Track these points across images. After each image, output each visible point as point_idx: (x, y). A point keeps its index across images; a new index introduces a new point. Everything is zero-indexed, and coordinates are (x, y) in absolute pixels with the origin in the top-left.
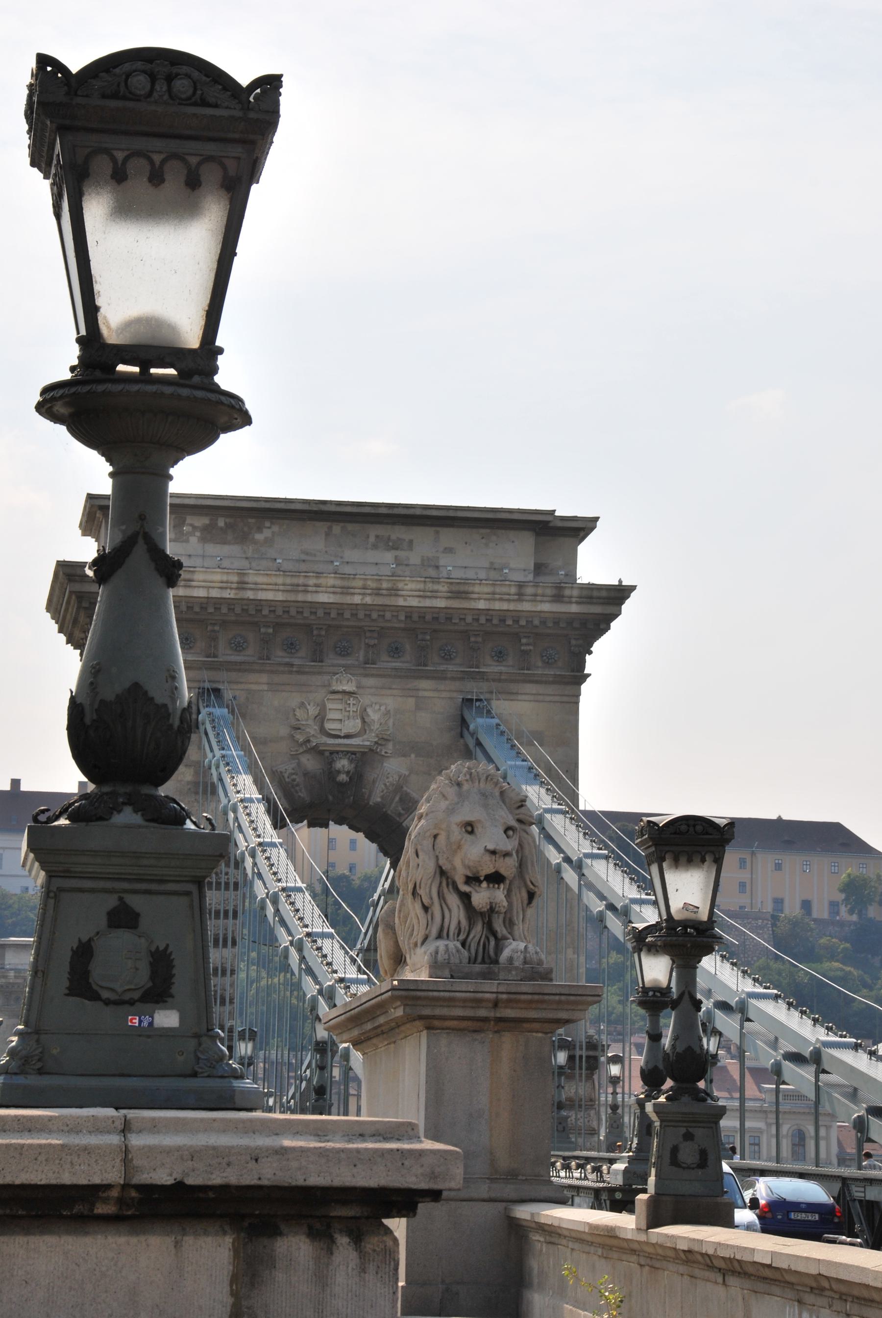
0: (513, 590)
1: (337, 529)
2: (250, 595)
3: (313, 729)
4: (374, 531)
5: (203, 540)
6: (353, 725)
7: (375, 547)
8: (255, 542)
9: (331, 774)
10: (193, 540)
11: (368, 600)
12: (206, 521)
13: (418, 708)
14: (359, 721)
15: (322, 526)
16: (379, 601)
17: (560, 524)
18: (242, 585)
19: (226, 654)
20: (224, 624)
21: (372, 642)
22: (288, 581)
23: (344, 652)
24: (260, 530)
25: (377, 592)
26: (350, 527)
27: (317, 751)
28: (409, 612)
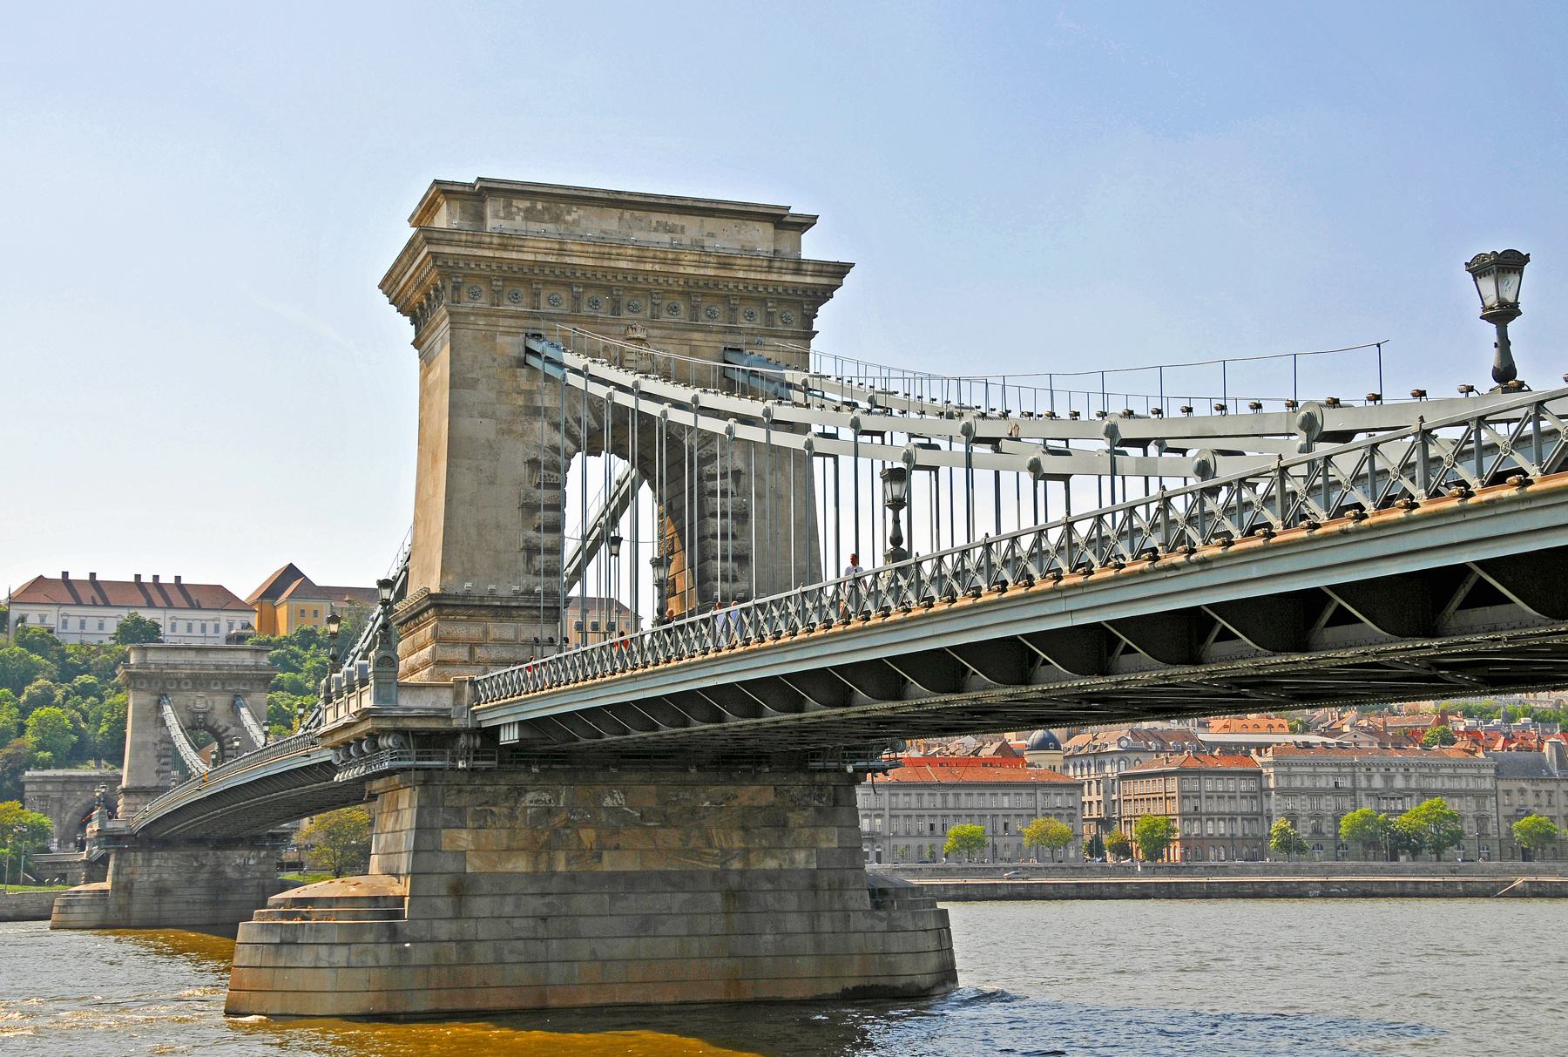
1: (627, 214)
2: (568, 260)
4: (656, 217)
5: (526, 219)
7: (656, 230)
10: (518, 218)
11: (657, 267)
12: (527, 204)
15: (616, 212)
16: (666, 268)
18: (561, 252)
19: (545, 307)
20: (545, 282)
23: (634, 309)
24: (569, 213)
25: (664, 261)
26: (637, 213)
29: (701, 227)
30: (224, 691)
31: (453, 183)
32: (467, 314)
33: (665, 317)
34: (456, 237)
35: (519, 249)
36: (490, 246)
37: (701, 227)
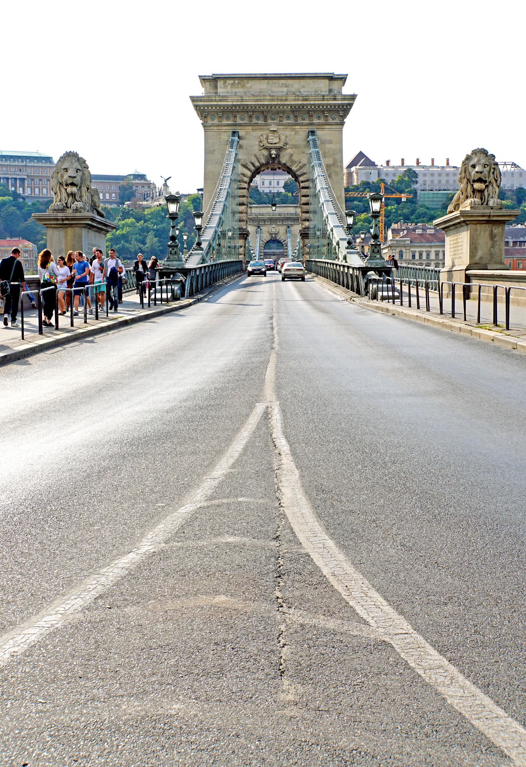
0: (321, 98)
1: (270, 81)
2: (245, 103)
3: (265, 142)
5: (232, 87)
6: (276, 140)
7: (282, 87)
8: (246, 87)
9: (270, 155)
10: (229, 87)
11: (279, 103)
13: (295, 134)
14: (278, 139)
15: (266, 81)
16: (282, 103)
17: (336, 77)
19: (239, 121)
21: (281, 115)
22: (255, 98)
24: (248, 83)
25: (281, 100)
26: (274, 81)
27: (266, 148)
28: (291, 106)
29: (300, 83)
30: (283, 225)
31: (205, 76)
32: (210, 126)
33: (285, 121)
34: (203, 99)
35: (226, 101)
36: (215, 101)
37: (300, 83)
